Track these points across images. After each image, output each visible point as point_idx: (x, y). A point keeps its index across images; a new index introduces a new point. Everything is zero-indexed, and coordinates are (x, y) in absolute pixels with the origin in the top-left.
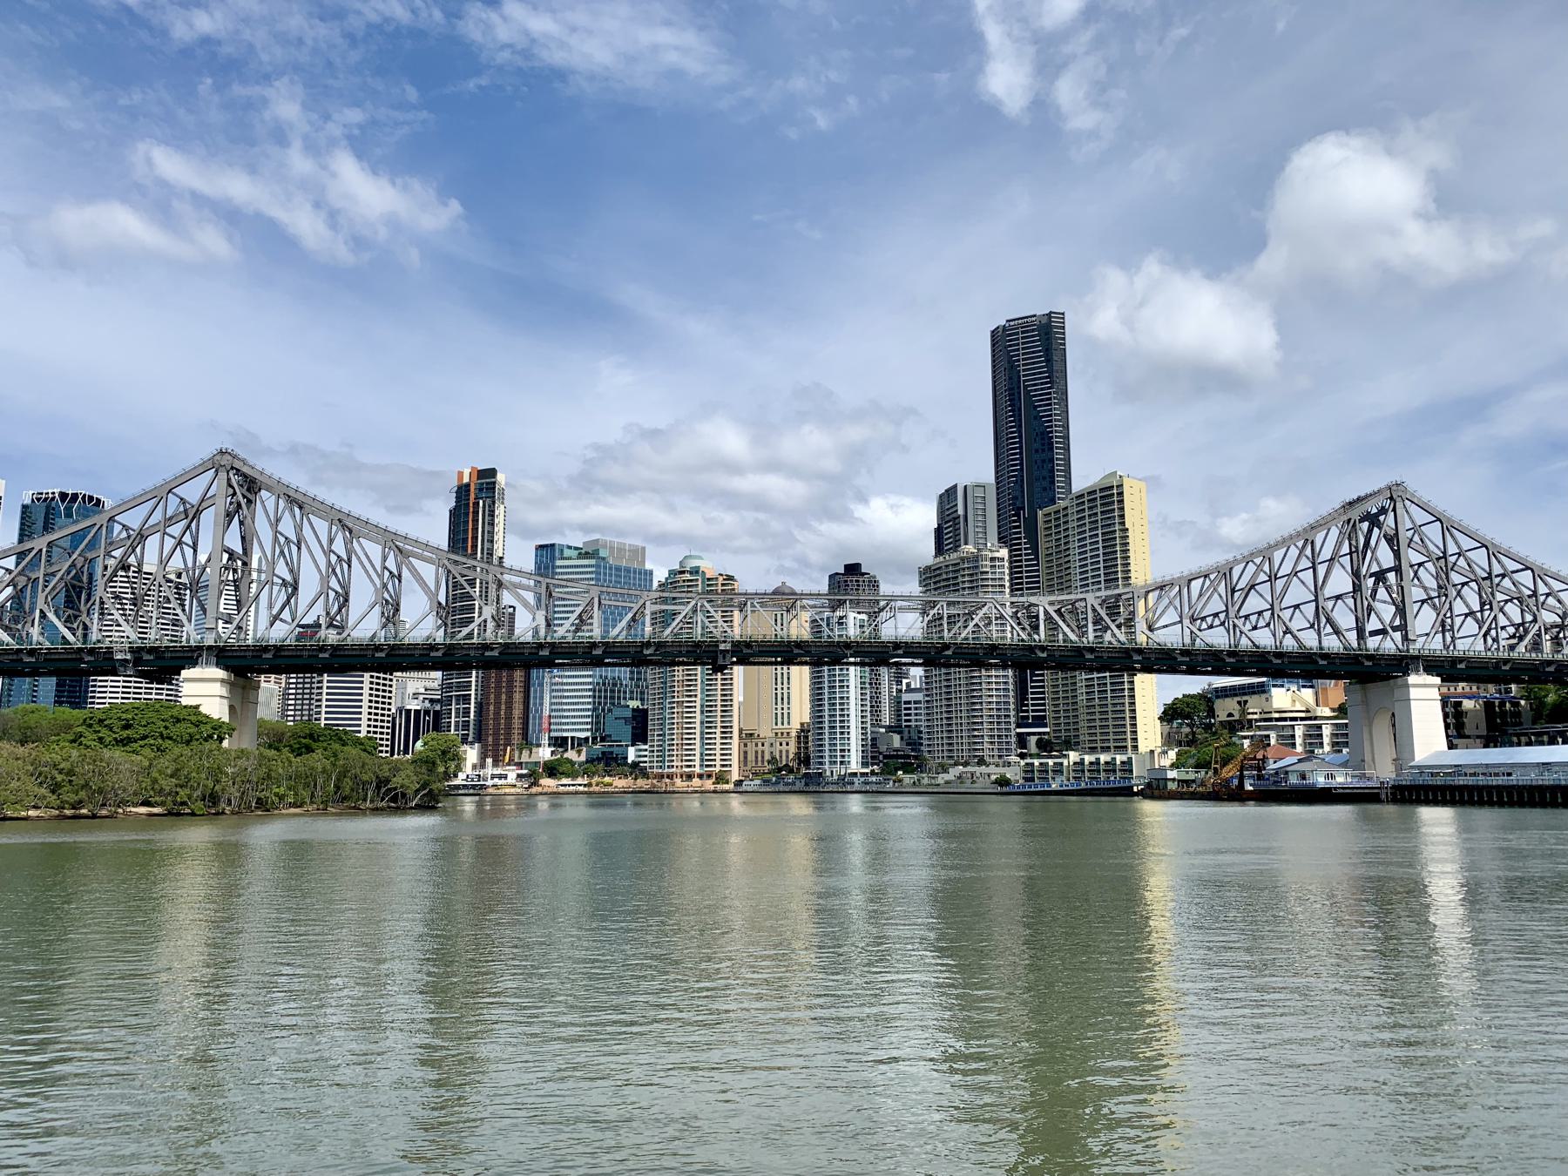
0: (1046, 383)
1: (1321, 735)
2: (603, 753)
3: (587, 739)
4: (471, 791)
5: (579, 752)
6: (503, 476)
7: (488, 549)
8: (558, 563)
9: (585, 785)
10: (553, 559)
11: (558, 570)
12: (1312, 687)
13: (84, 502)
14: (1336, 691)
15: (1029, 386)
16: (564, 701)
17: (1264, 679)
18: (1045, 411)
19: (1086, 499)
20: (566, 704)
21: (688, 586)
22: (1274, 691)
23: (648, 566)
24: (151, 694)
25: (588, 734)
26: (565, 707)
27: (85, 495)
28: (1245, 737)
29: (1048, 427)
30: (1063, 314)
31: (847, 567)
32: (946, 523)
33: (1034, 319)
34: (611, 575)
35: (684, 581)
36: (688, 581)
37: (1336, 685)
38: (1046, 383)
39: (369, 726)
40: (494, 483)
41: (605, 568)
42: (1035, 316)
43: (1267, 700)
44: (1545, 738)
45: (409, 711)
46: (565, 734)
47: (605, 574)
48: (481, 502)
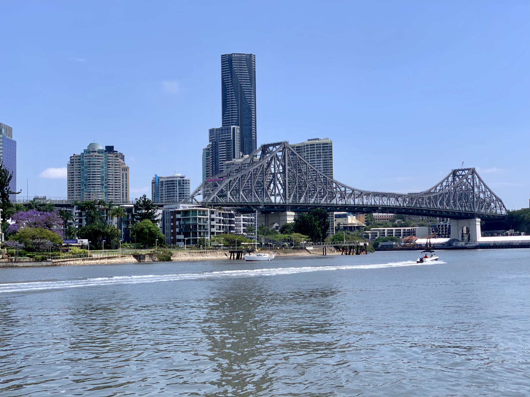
0: (249, 84)
1: (393, 232)
12: (355, 216)
14: (363, 217)
15: (242, 84)
17: (346, 213)
18: (248, 96)
19: (316, 146)
21: (98, 159)
22: (349, 217)
23: (14, 138)
28: (368, 233)
29: (250, 103)
30: (255, 56)
31: (107, 147)
32: (220, 142)
33: (245, 56)
35: (96, 156)
37: (363, 215)
38: (249, 84)
42: (245, 54)
43: (346, 220)
44: (490, 234)
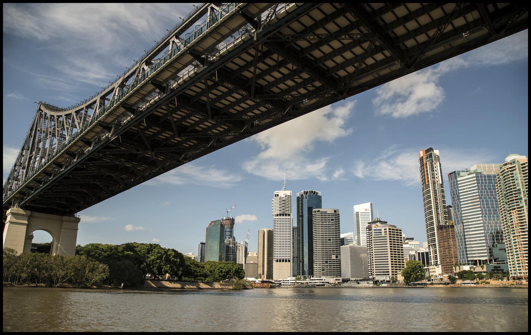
2: (495, 267)
3: (486, 260)
4: (421, 286)
5: (482, 267)
6: (438, 151)
7: (433, 181)
8: (458, 179)
9: (475, 283)
10: (456, 178)
11: (459, 183)
13: (310, 193)
16: (472, 243)
20: (473, 244)
24: (331, 252)
25: (487, 258)
26: (473, 246)
27: (310, 191)
34: (485, 180)
35: (508, 169)
36: (510, 168)
39: (403, 260)
40: (432, 153)
41: (481, 177)
45: (419, 253)
46: (475, 259)
47: (482, 180)
48: (428, 162)
